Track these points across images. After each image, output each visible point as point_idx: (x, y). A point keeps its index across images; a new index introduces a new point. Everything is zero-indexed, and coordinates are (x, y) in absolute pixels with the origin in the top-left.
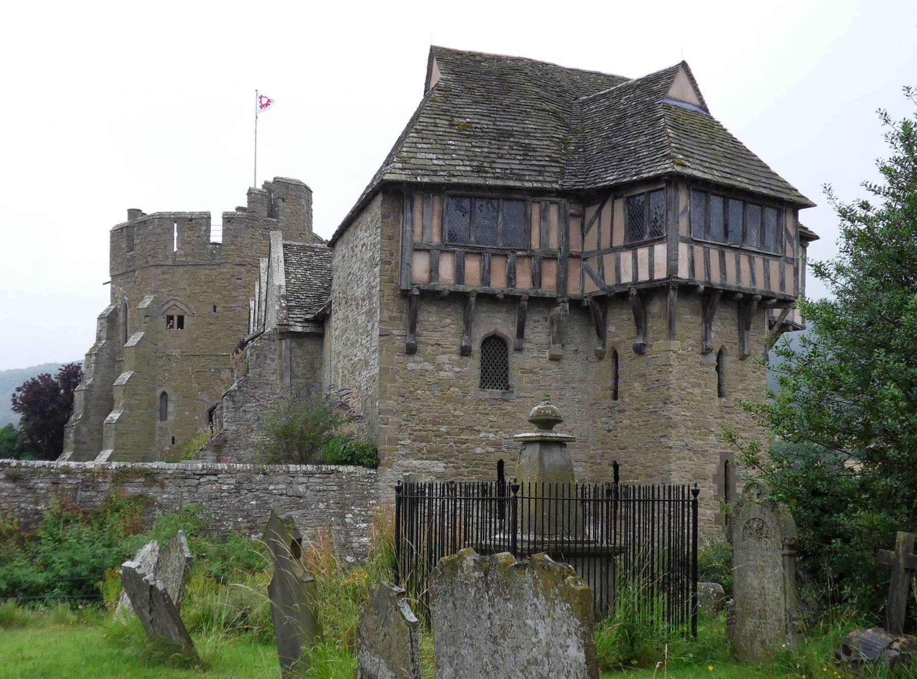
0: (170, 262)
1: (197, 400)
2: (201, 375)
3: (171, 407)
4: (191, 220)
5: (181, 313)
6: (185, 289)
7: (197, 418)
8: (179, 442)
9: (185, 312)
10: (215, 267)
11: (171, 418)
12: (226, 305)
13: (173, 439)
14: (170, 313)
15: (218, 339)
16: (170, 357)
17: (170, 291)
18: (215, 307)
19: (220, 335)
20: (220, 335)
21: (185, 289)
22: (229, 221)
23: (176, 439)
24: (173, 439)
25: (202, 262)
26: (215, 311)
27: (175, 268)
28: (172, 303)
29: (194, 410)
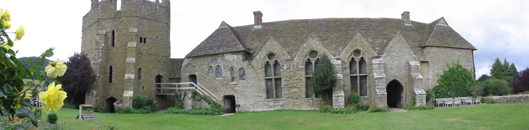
0: (142, 16)
1: (152, 72)
2: (154, 63)
3: (142, 74)
4: (149, 3)
5: (145, 37)
6: (147, 28)
7: (152, 79)
8: (145, 88)
9: (147, 37)
10: (157, 22)
11: (142, 78)
12: (161, 37)
13: (143, 87)
14: (142, 36)
15: (159, 49)
16: (142, 54)
17: (142, 27)
18: (157, 37)
19: (160, 48)
20: (160, 48)
21: (147, 28)
22: (161, 7)
23: (145, 86)
24: (143, 87)
25: (153, 19)
26: (157, 39)
27: (144, 19)
28: (143, 32)
29: (151, 76)
